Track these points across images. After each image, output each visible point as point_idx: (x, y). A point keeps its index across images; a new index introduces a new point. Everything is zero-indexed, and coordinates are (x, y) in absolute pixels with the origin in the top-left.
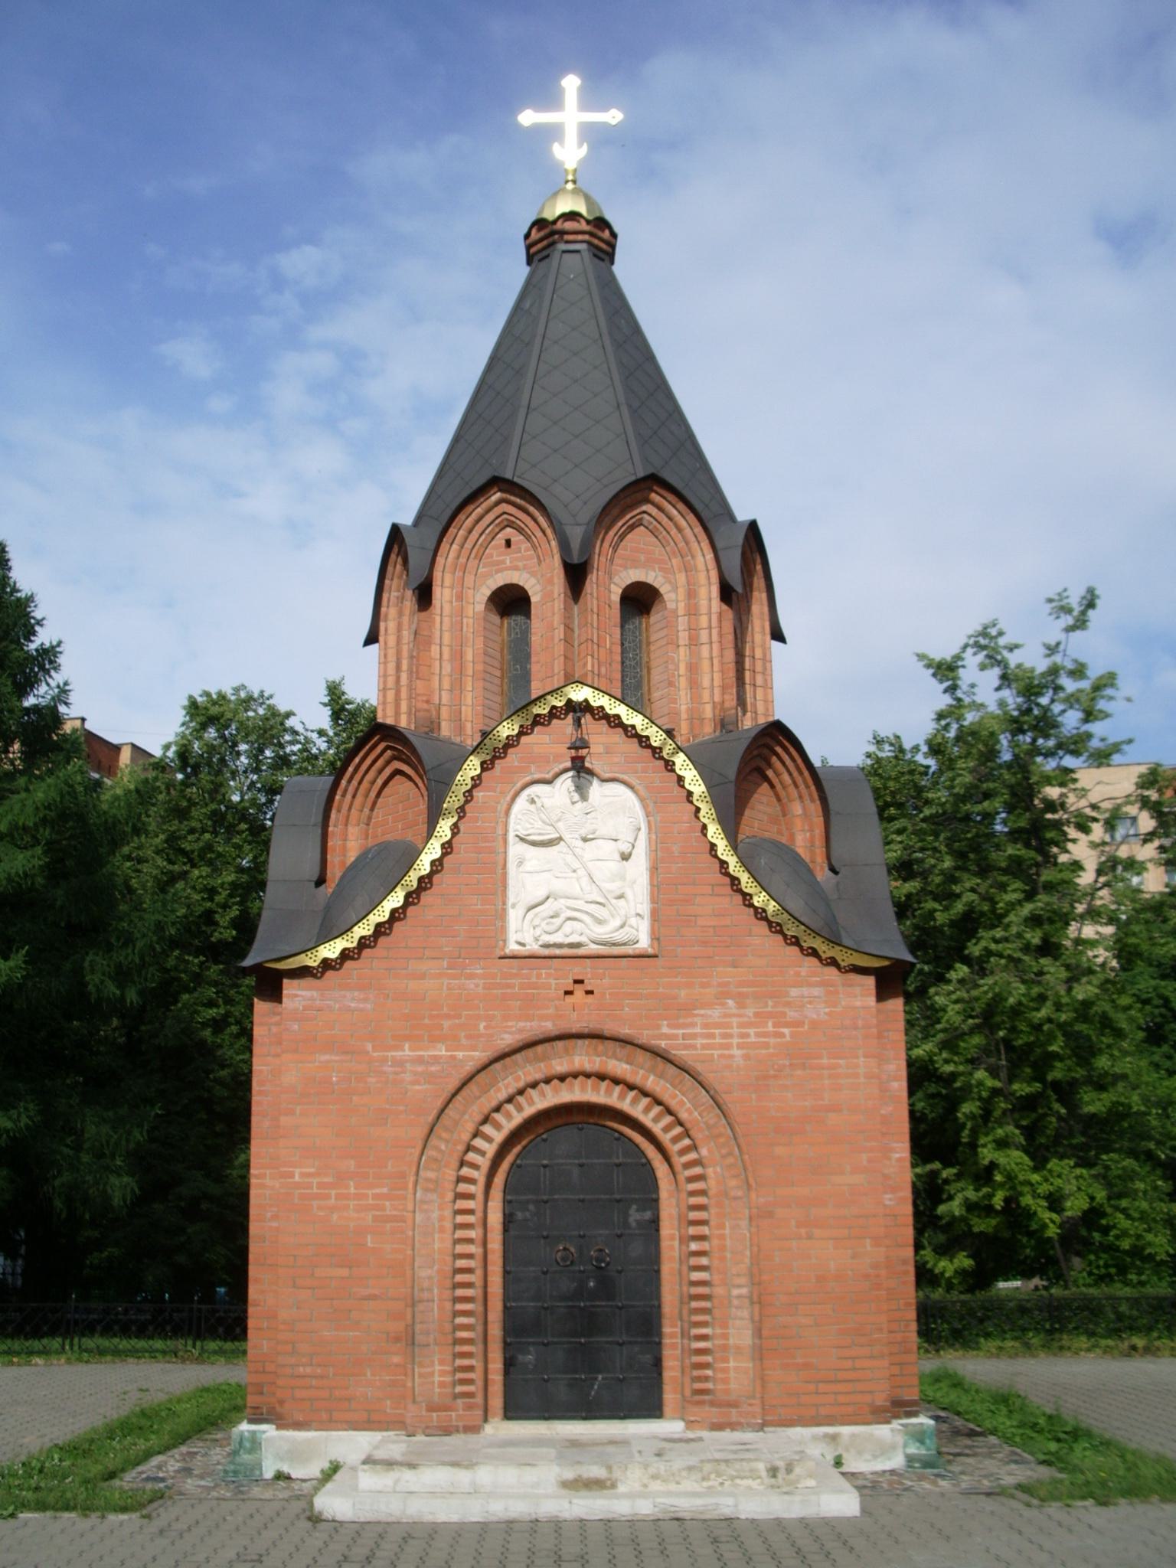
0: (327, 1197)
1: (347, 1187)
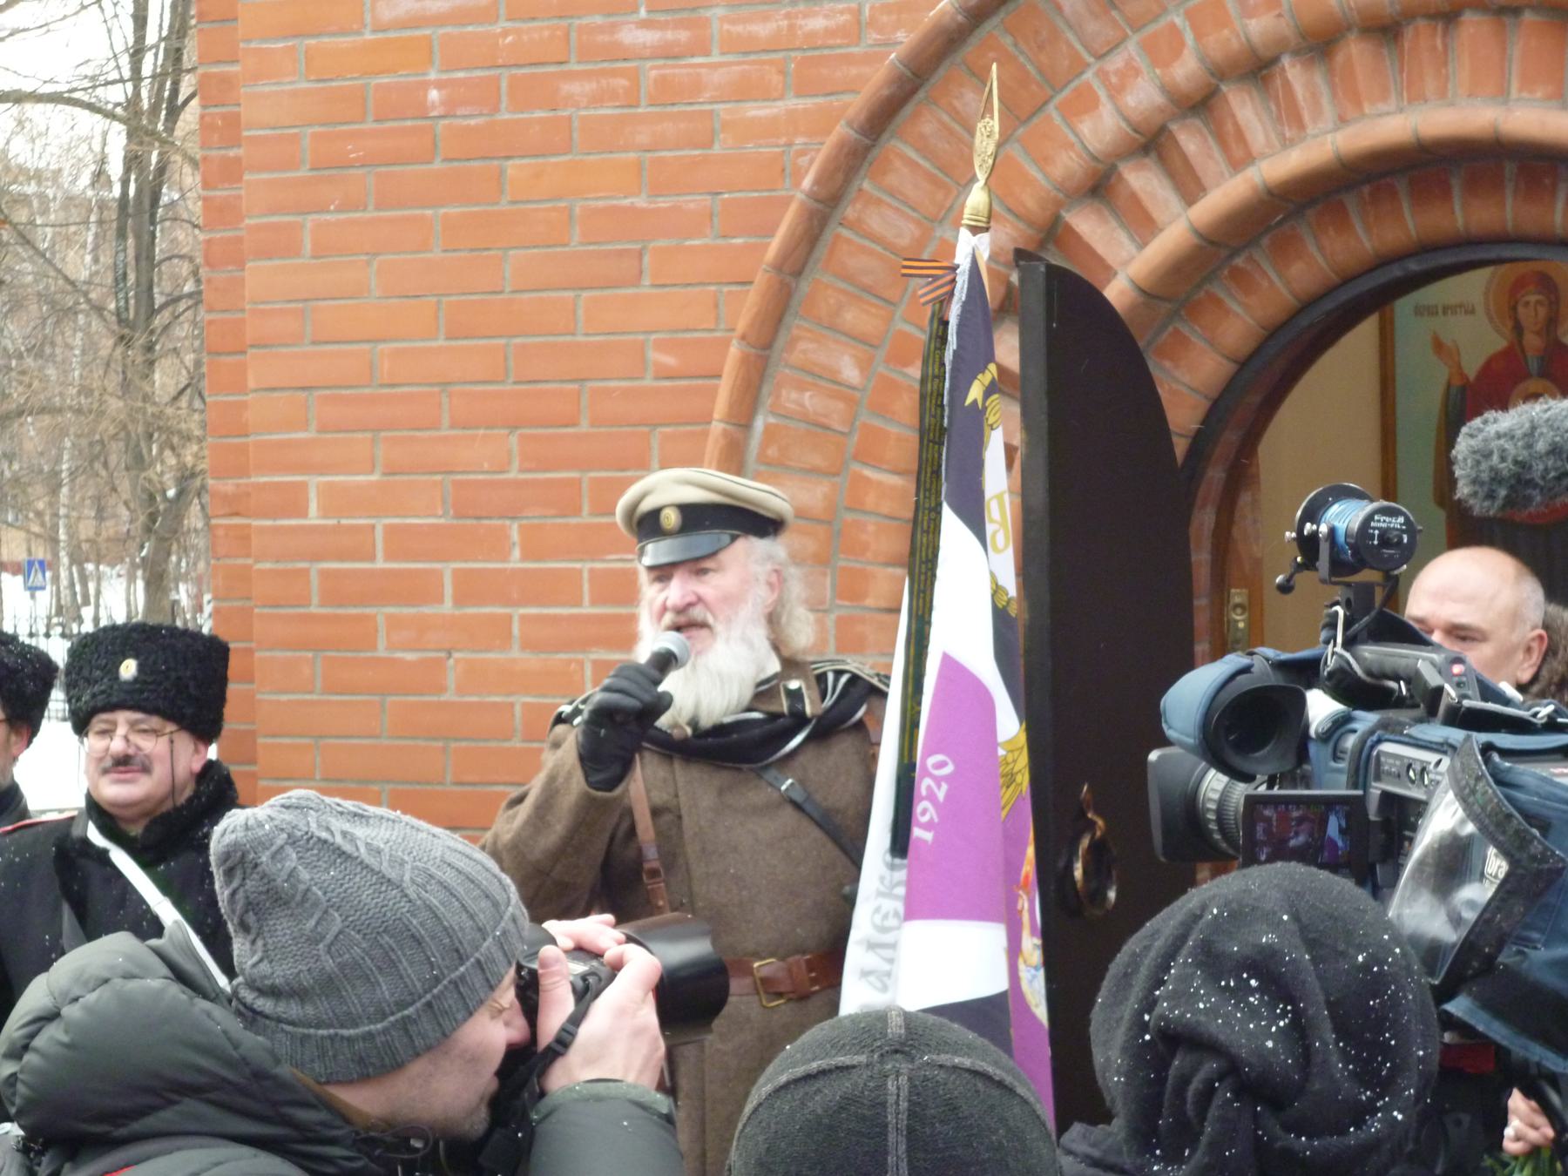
0: (424, 590)
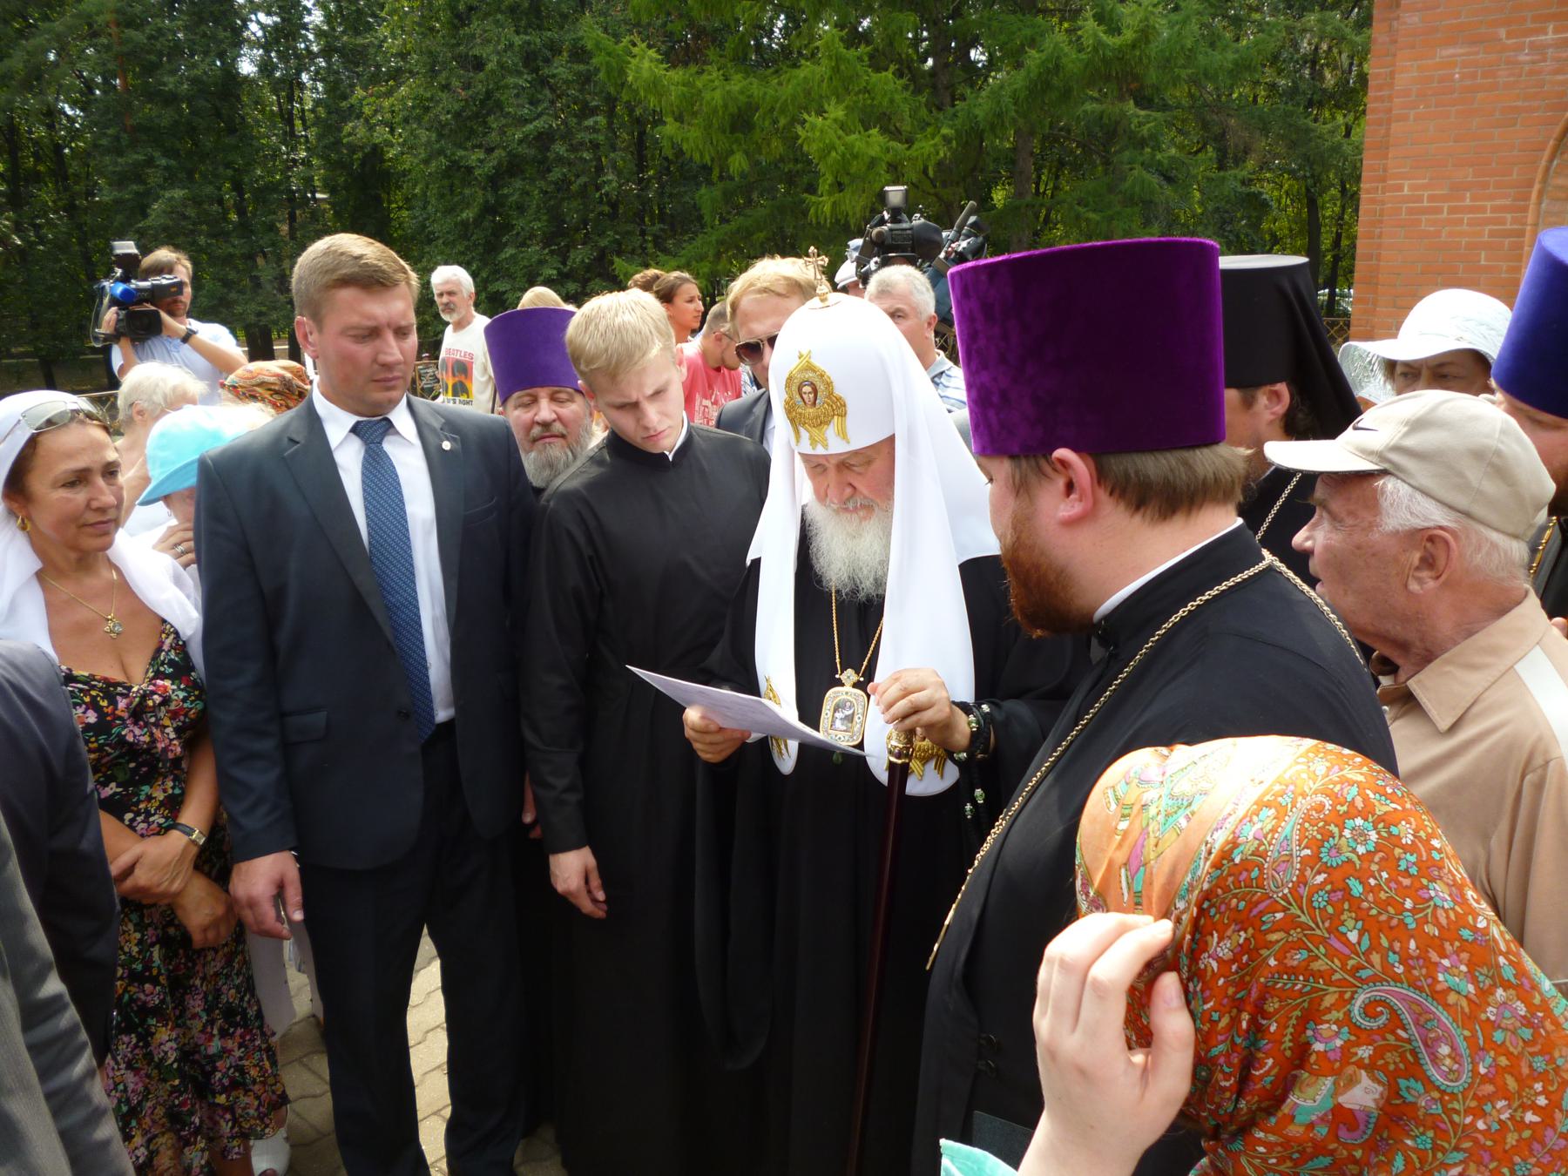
0: (1439, 210)
1: (1464, 199)
